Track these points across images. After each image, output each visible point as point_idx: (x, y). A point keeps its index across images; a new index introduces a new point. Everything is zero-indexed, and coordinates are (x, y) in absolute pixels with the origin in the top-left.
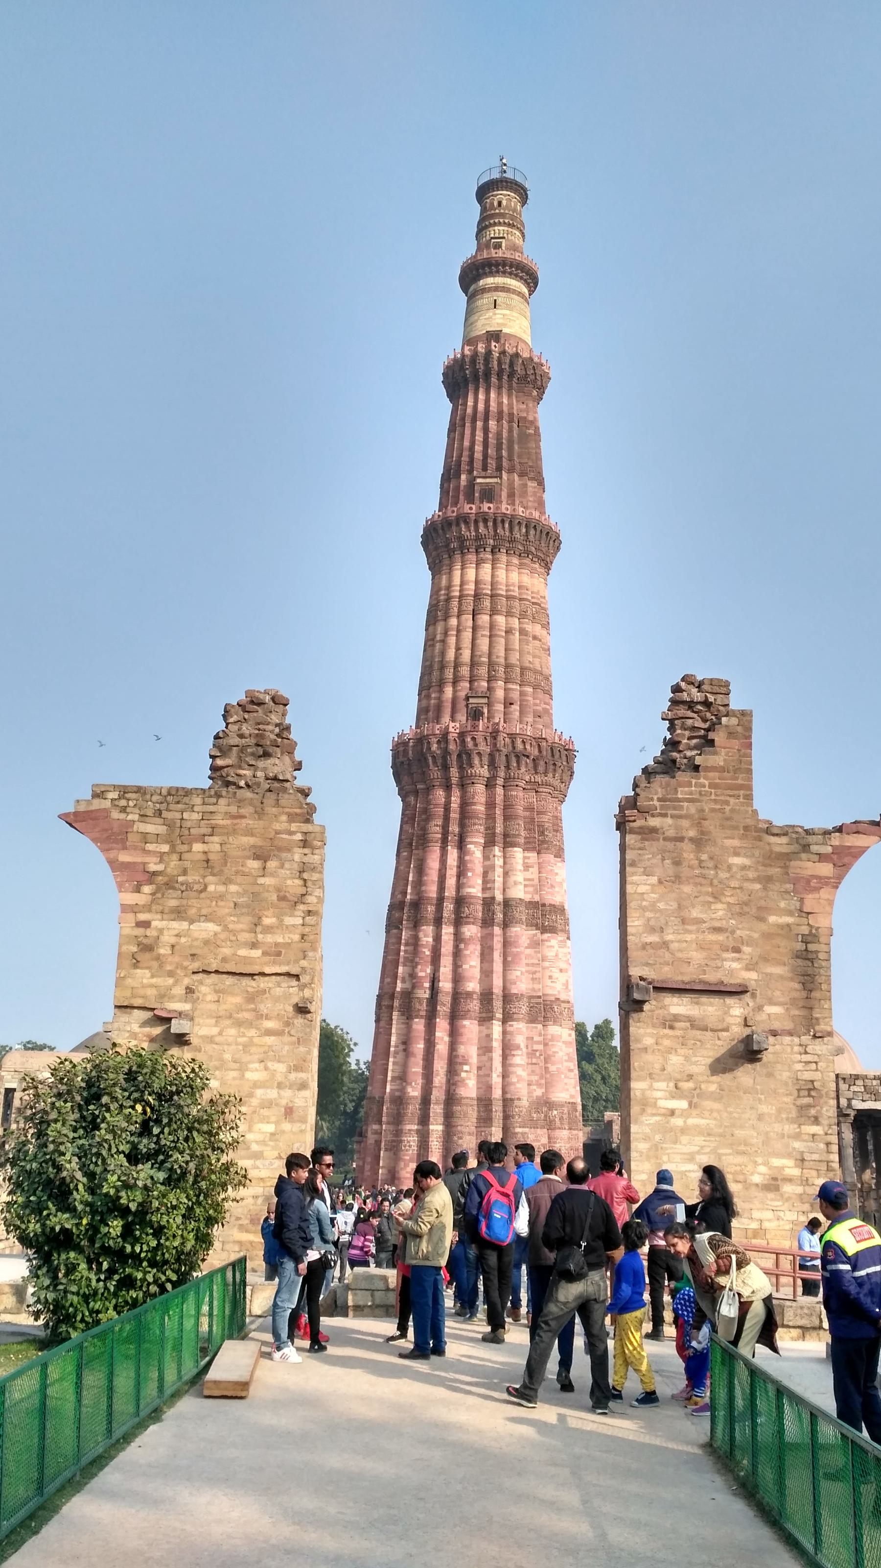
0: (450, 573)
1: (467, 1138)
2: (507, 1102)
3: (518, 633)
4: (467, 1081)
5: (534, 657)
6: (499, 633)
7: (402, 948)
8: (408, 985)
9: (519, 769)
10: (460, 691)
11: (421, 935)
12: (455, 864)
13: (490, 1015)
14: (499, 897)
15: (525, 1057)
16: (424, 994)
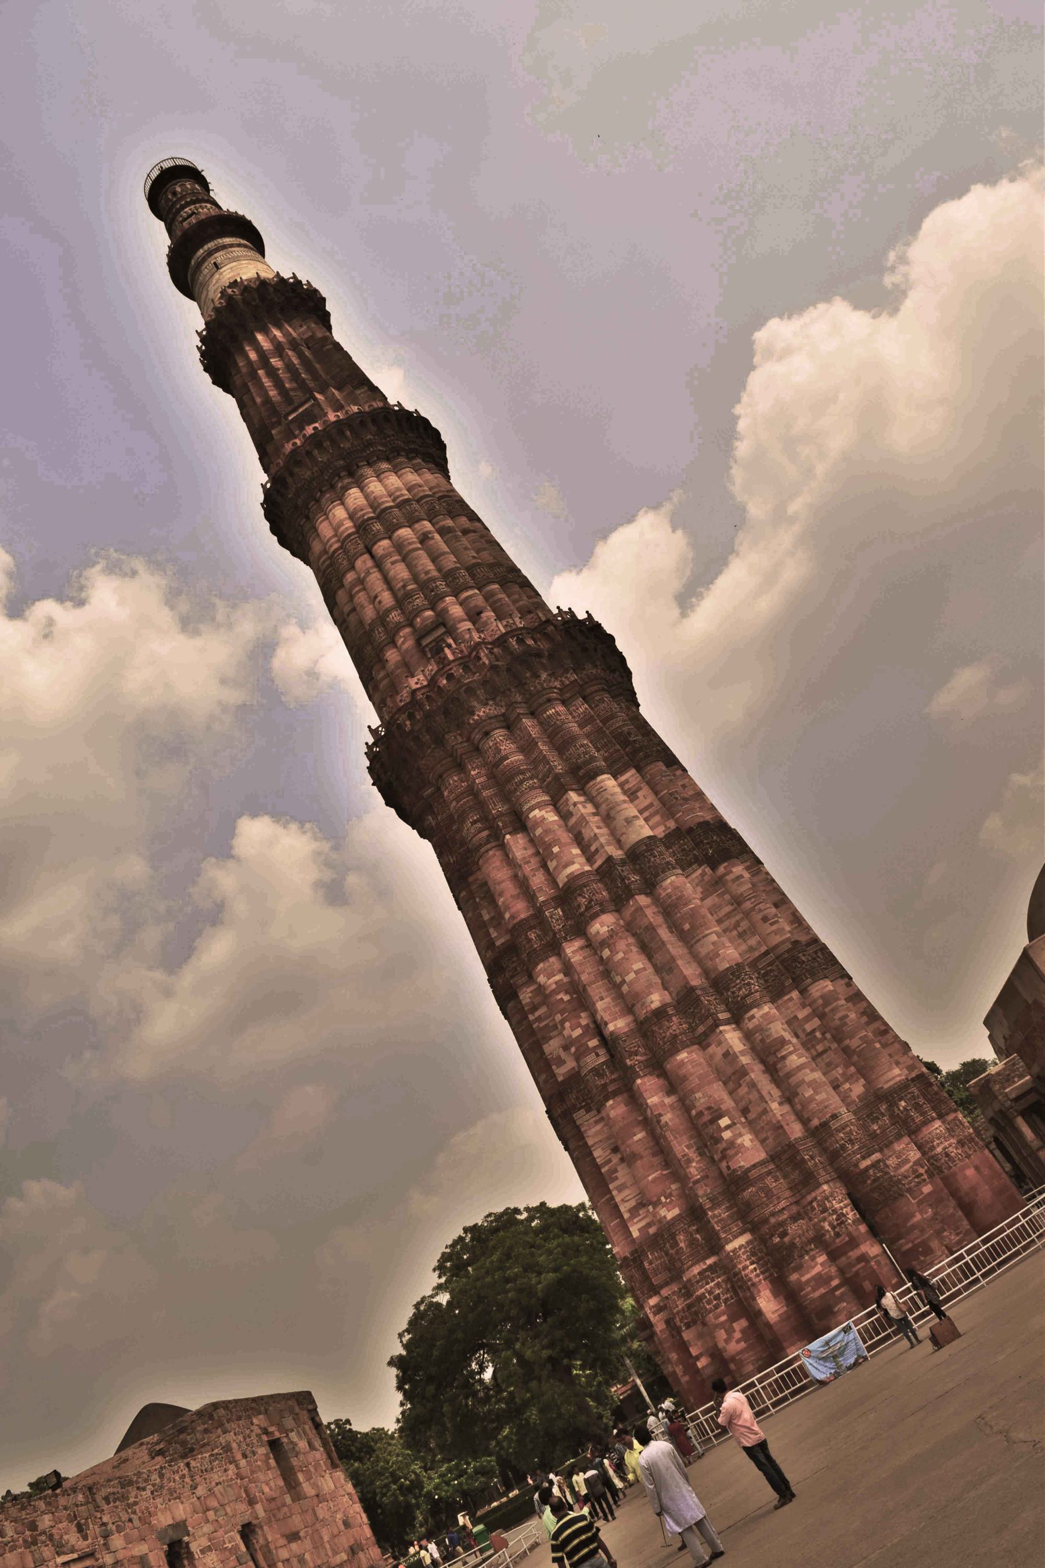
0: (318, 535)
1: (793, 1229)
2: (820, 1132)
3: (437, 536)
4: (739, 1141)
5: (478, 552)
6: (411, 547)
7: (531, 1017)
8: (570, 1064)
9: (538, 677)
10: (403, 643)
11: (542, 979)
12: (531, 851)
13: (710, 1021)
14: (618, 854)
15: (802, 1051)
16: (596, 1059)
